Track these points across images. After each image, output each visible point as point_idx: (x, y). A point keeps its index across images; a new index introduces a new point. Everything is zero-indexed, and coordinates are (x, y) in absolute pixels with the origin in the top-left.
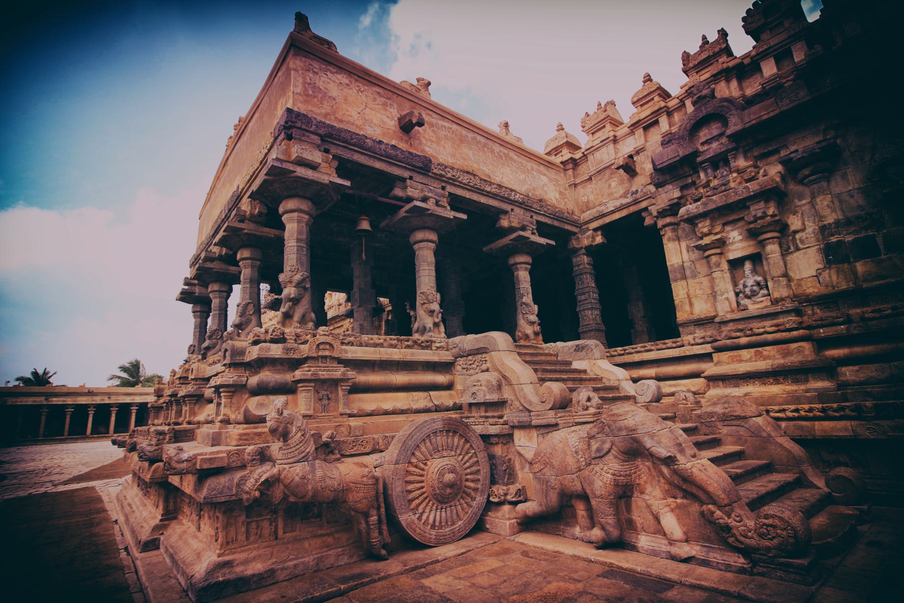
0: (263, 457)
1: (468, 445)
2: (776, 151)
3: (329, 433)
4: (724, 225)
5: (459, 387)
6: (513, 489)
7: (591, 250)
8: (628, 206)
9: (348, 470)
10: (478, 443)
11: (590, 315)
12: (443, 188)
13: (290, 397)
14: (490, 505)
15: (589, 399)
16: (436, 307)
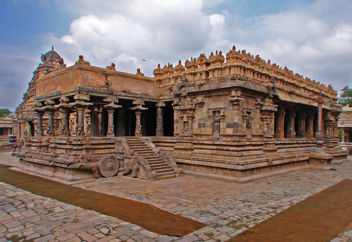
0: (79, 162)
1: (115, 161)
2: (195, 98)
3: (89, 158)
4: (184, 113)
5: (116, 148)
6: (123, 169)
7: (162, 107)
8: (170, 99)
9: (93, 164)
10: (117, 161)
11: (160, 127)
12: (117, 97)
13: (81, 151)
14: (118, 172)
15: (136, 154)
16: (112, 129)
